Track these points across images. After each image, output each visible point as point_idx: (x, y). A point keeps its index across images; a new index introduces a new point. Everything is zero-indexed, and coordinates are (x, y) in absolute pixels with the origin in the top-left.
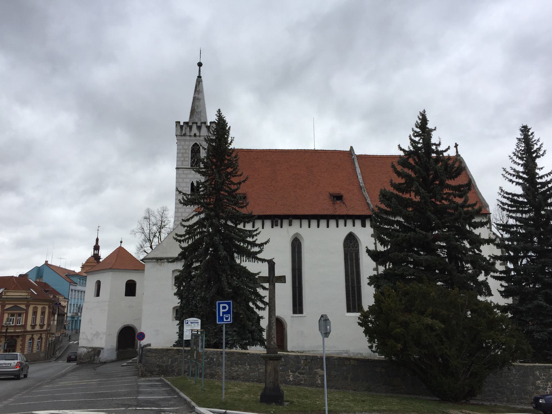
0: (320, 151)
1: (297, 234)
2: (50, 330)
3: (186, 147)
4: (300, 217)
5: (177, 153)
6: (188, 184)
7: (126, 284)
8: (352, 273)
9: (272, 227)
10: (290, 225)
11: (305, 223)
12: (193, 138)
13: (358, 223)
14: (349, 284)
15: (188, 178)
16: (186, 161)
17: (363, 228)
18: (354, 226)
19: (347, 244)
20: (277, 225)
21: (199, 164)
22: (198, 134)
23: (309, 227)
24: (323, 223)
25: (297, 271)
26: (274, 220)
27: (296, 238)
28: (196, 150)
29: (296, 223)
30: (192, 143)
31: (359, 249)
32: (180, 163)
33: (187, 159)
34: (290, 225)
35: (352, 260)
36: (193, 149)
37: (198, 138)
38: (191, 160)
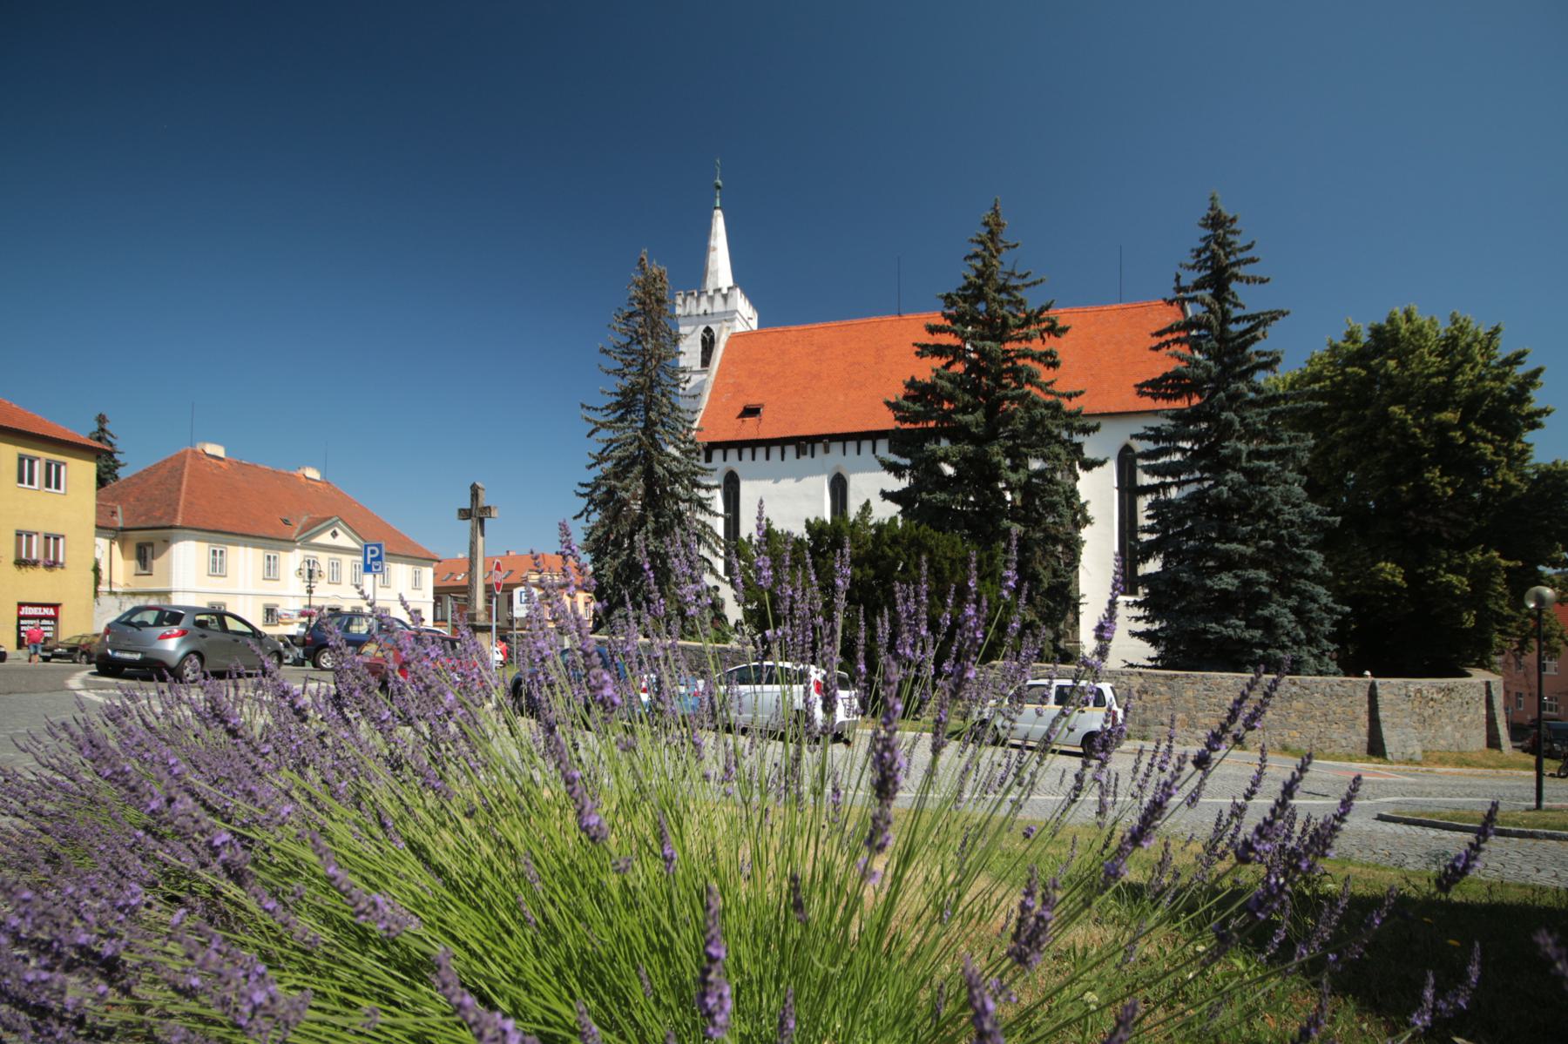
9: (798, 457)
10: (827, 450)
11: (851, 446)
20: (805, 454)
22: (709, 311)
29: (836, 447)
30: (702, 327)
37: (710, 319)
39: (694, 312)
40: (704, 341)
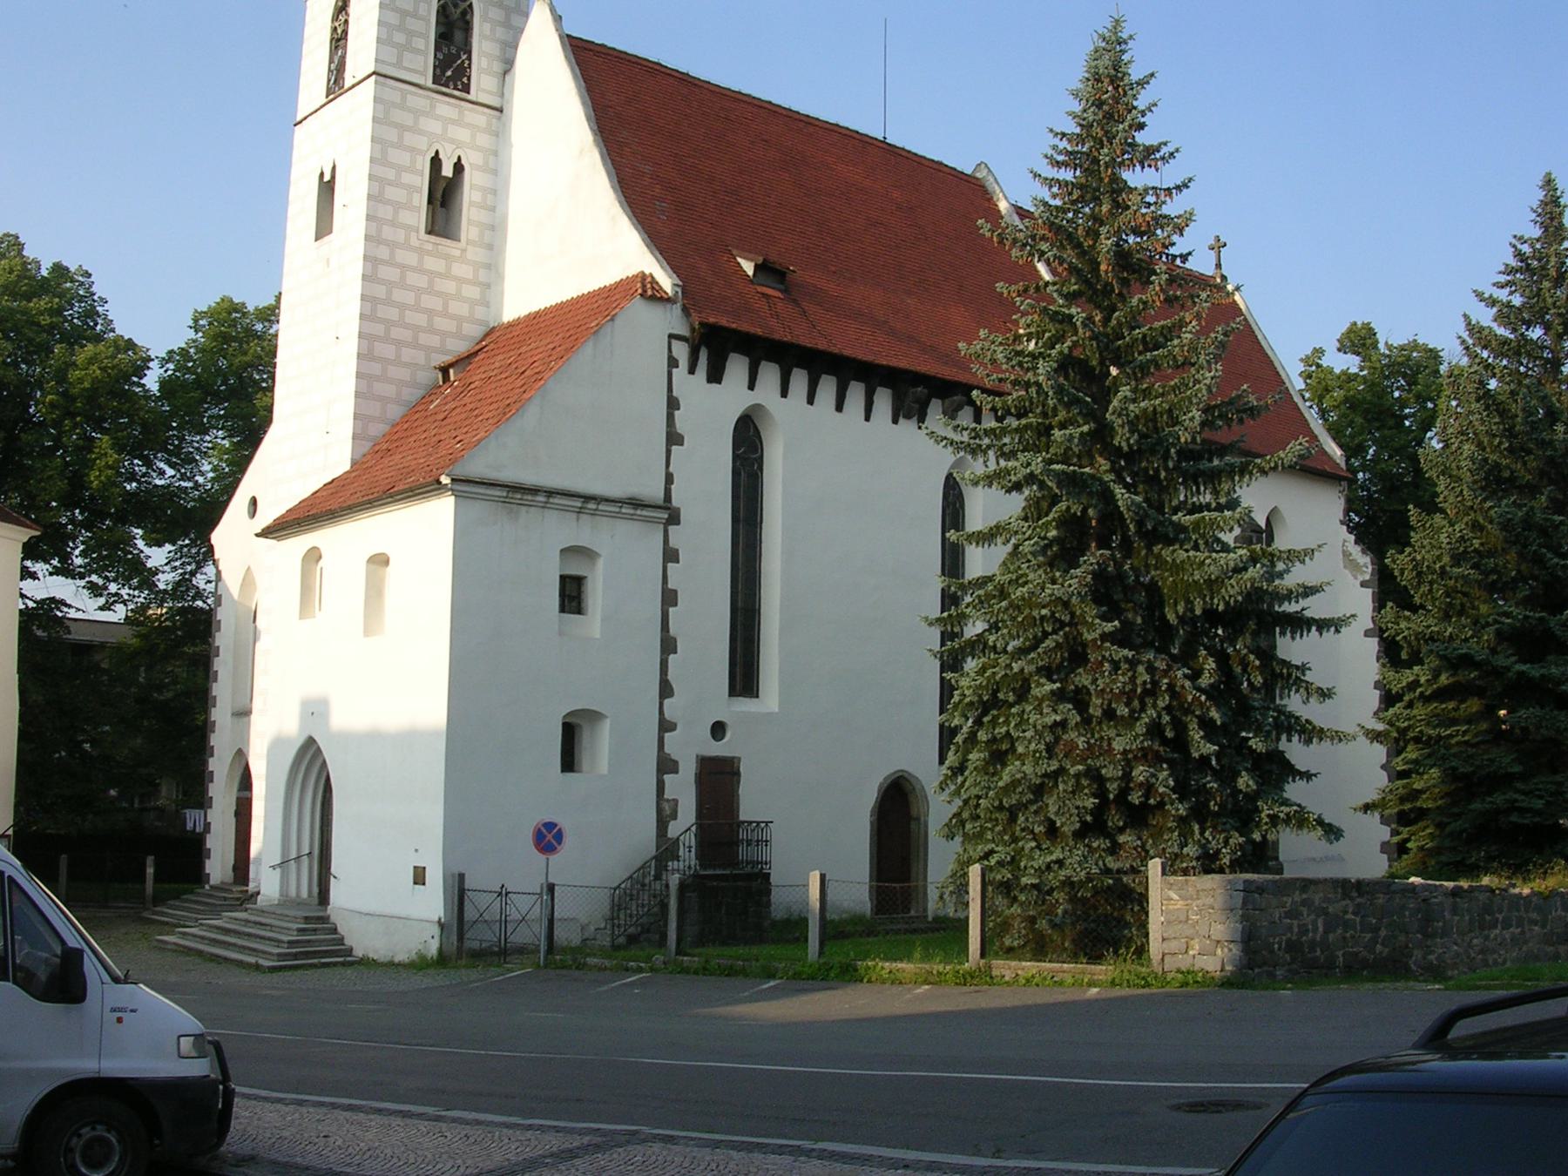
6: (419, 159)
15: (422, 133)
16: (417, 51)
21: (465, 80)
32: (391, 54)
33: (419, 43)
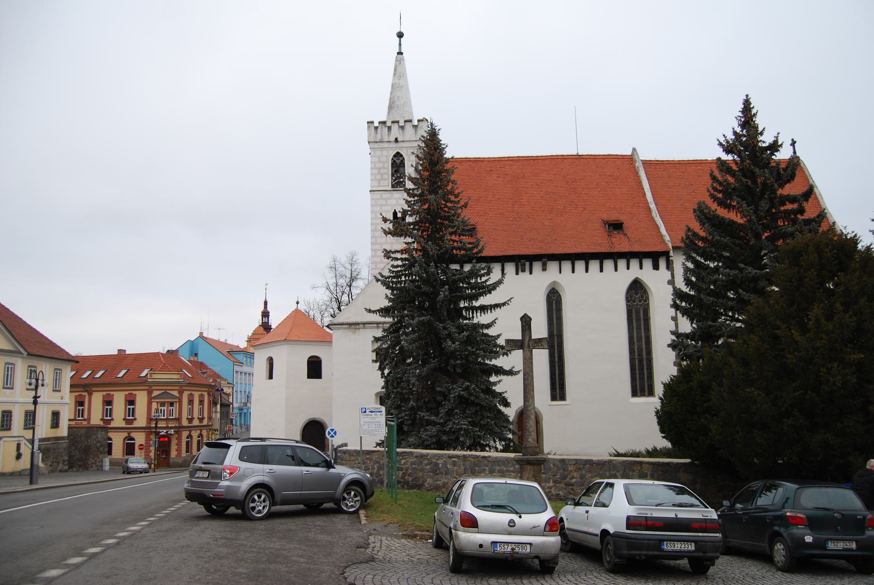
0: (586, 157)
1: (555, 282)
2: (211, 425)
3: (384, 159)
4: (559, 258)
5: (371, 168)
7: (308, 361)
8: (639, 339)
9: (517, 274)
10: (544, 269)
11: (567, 266)
12: (394, 145)
13: (648, 263)
14: (635, 356)
15: (389, 205)
16: (385, 179)
17: (655, 271)
18: (641, 268)
19: (631, 297)
20: (523, 271)
23: (573, 272)
24: (594, 265)
25: (556, 337)
26: (519, 263)
27: (553, 289)
28: (398, 162)
29: (553, 266)
31: (648, 304)
32: (376, 183)
33: (386, 177)
34: (544, 269)
35: (638, 320)
36: (394, 161)
37: (400, 144)
38: (392, 179)
39: (386, 139)
40: (394, 164)
